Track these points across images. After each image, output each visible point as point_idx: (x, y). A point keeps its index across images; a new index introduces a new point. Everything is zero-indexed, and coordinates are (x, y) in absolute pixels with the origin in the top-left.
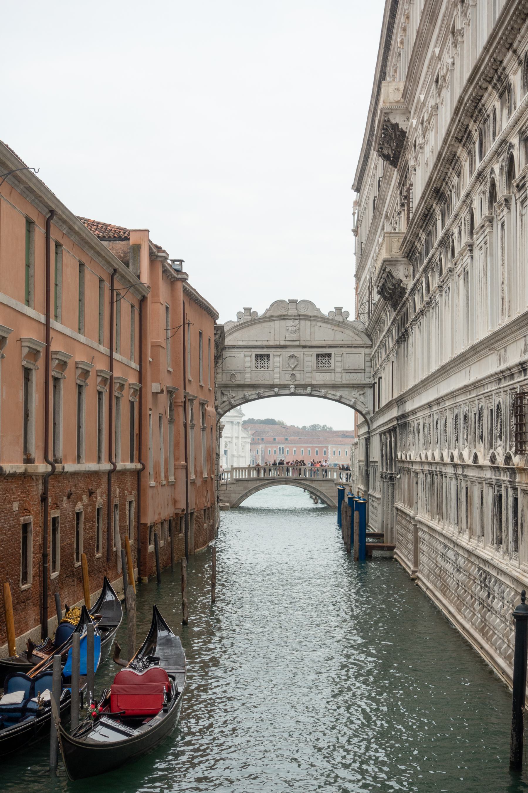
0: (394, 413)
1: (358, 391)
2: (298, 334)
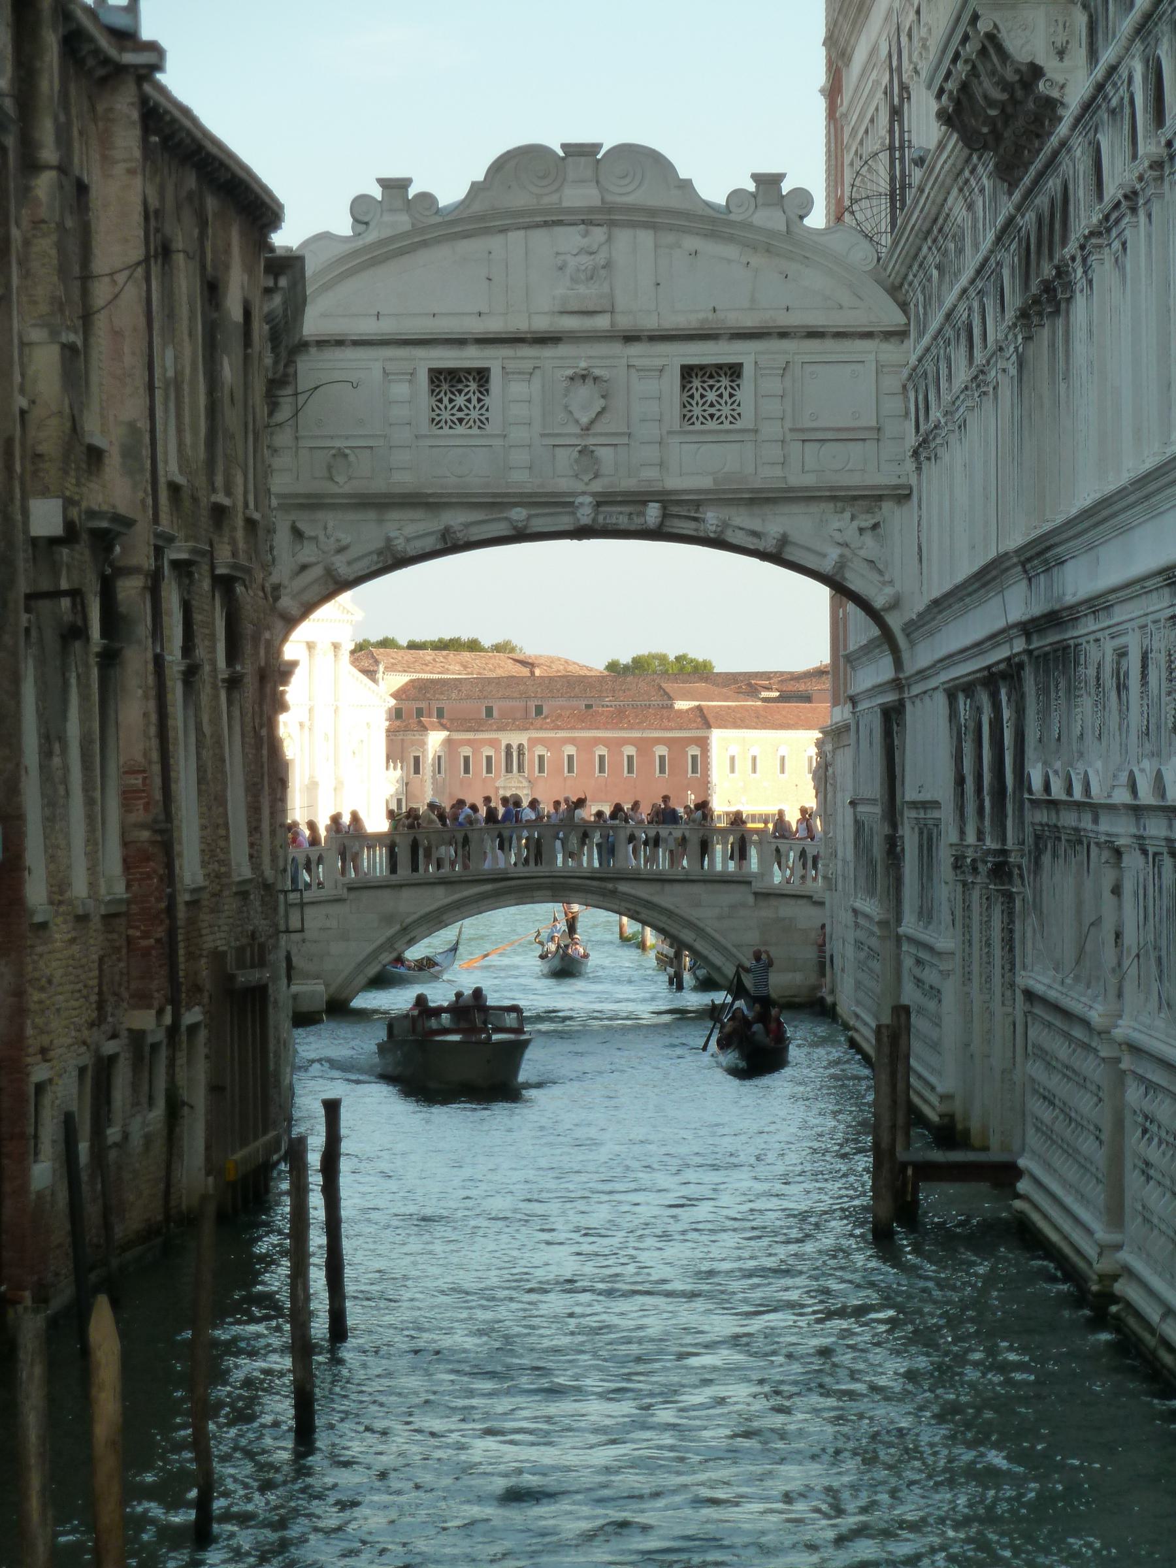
1: (853, 518)
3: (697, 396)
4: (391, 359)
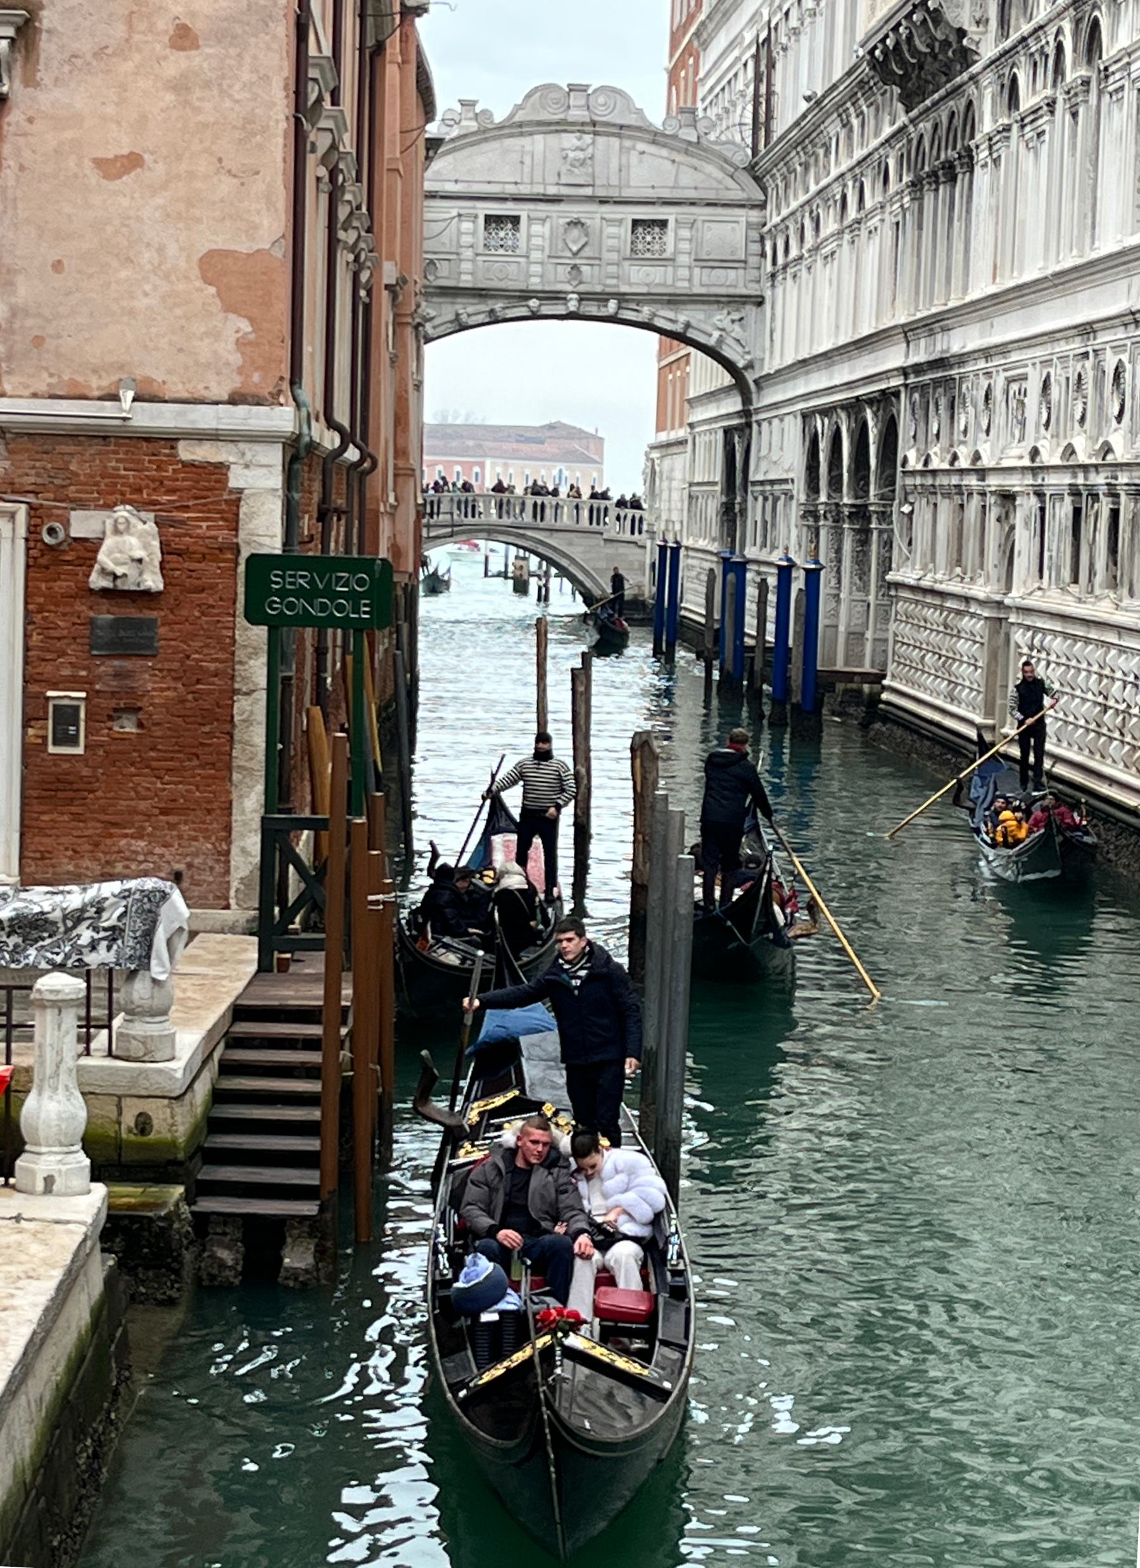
0: (894, 357)
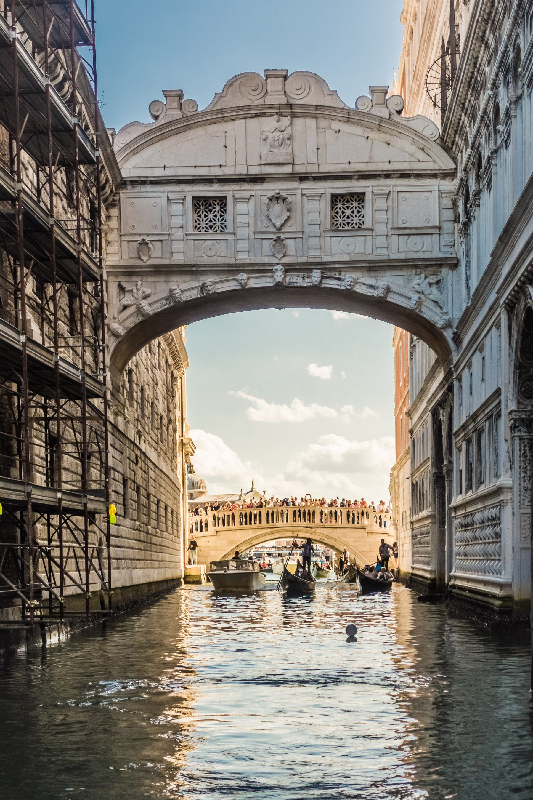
1: (426, 277)
2: (290, 150)
3: (340, 212)
4: (171, 192)
